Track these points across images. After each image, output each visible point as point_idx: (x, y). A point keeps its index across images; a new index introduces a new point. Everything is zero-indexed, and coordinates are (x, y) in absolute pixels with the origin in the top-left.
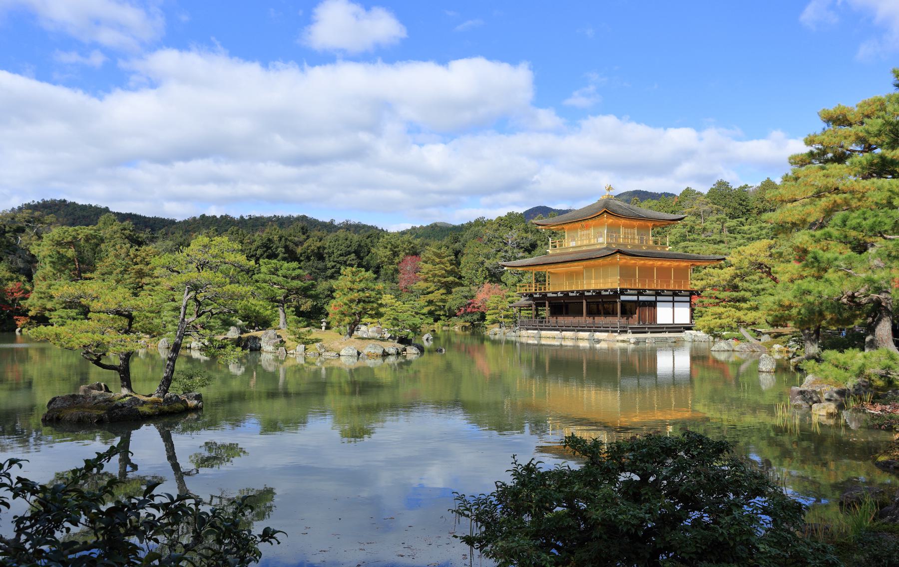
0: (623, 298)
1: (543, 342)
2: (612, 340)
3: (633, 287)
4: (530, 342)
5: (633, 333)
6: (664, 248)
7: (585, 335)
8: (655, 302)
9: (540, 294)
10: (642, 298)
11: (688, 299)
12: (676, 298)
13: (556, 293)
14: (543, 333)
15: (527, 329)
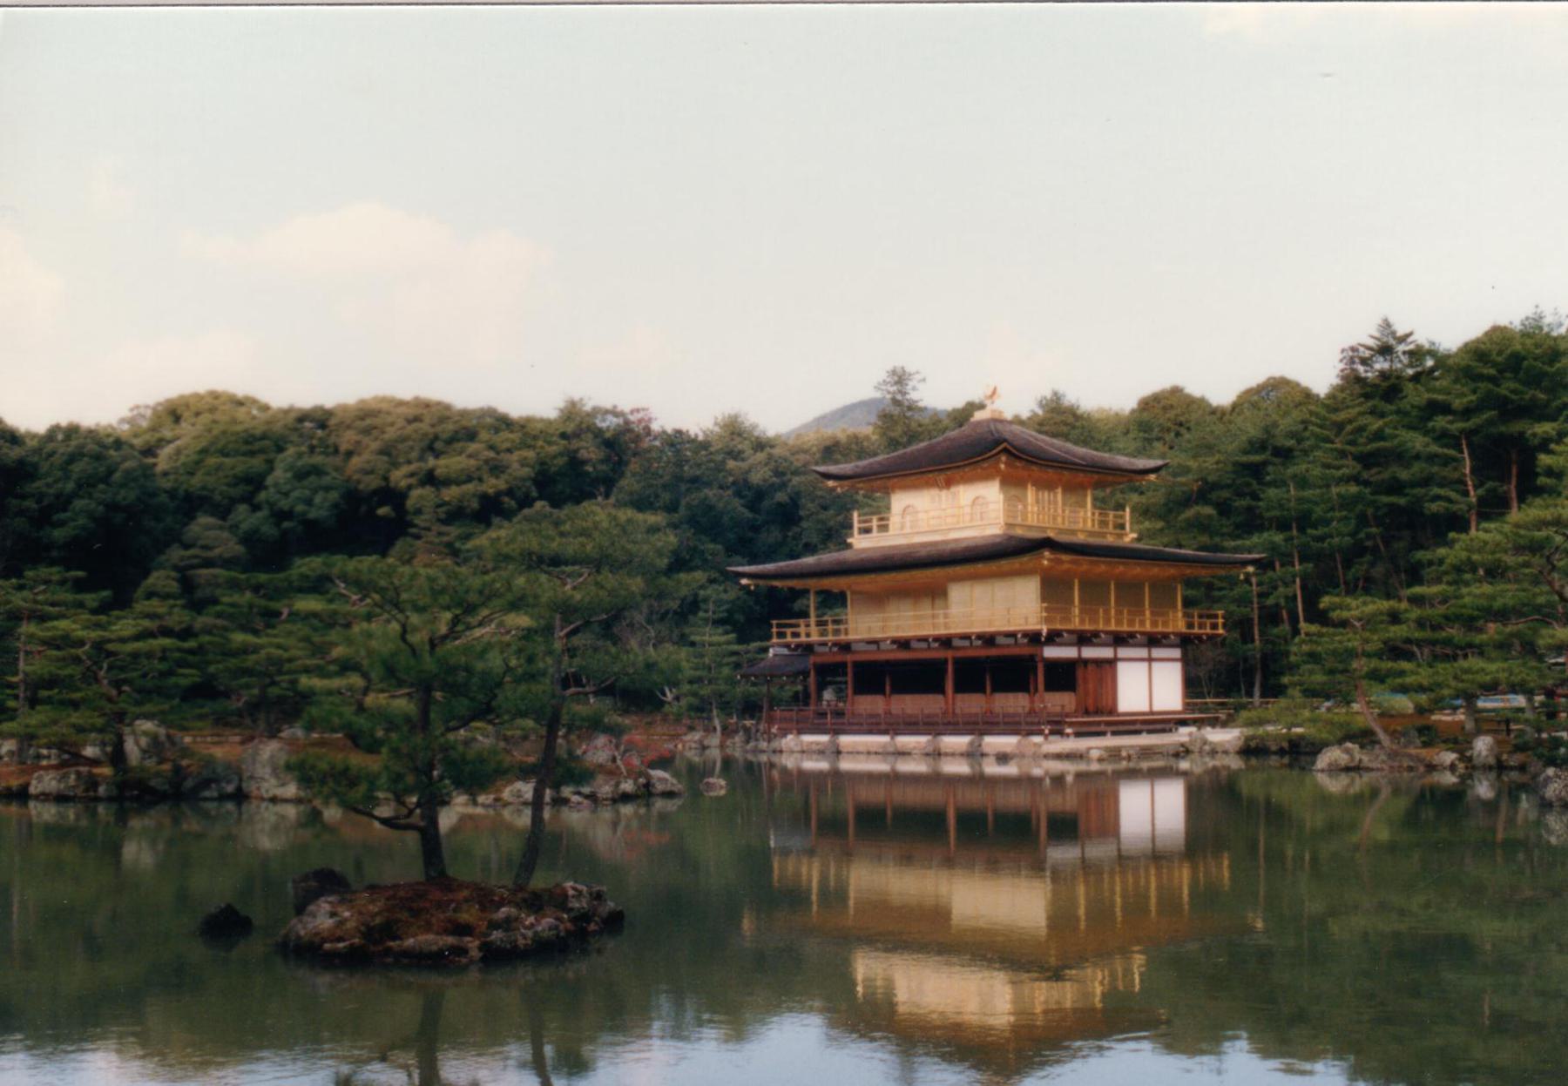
0: (1051, 652)
1: (846, 765)
2: (1017, 755)
3: (1071, 627)
4: (811, 765)
5: (1078, 735)
6: (1120, 536)
7: (960, 741)
8: (1112, 663)
9: (835, 644)
10: (1089, 653)
11: (1177, 653)
12: (1157, 652)
13: (875, 642)
14: (846, 740)
15: (800, 732)
